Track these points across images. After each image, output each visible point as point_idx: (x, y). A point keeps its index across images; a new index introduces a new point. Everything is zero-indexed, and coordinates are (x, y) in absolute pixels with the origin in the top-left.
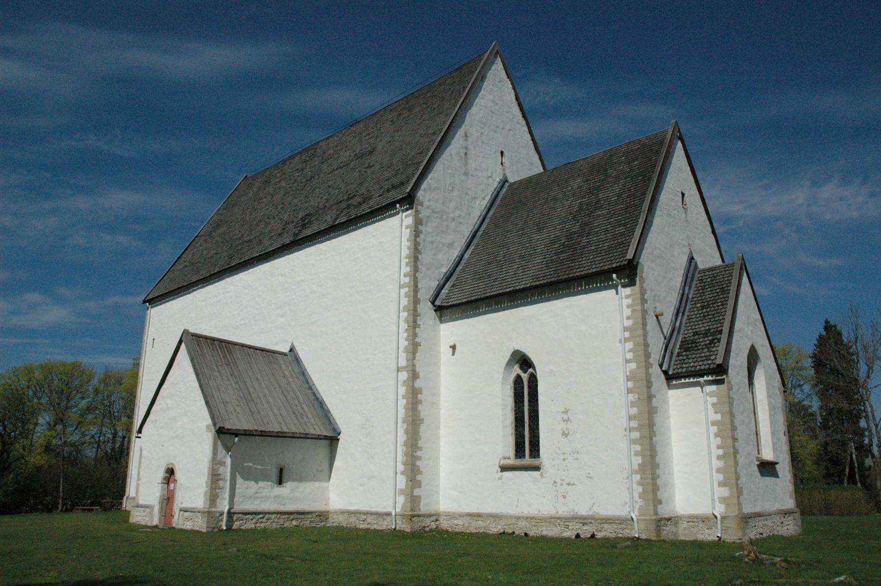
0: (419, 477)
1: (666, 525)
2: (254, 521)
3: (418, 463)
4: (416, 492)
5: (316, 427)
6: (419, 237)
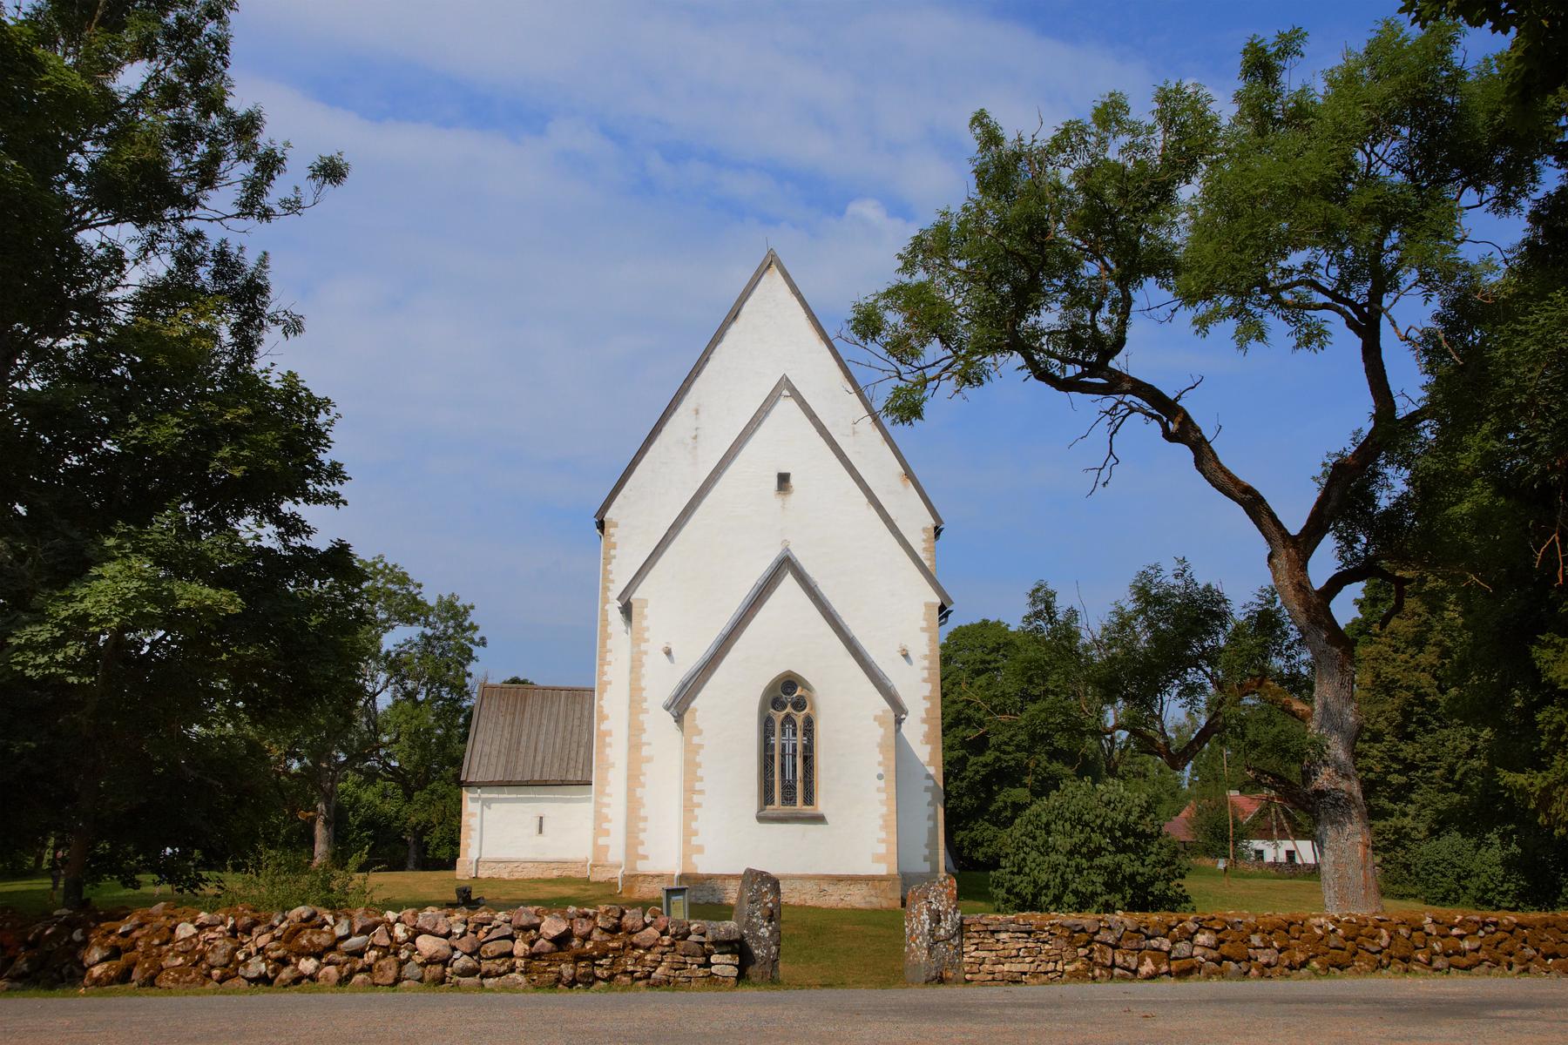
0: (606, 826)
1: (643, 881)
2: (508, 870)
3: (605, 810)
4: (602, 841)
5: (580, 773)
6: (610, 563)
